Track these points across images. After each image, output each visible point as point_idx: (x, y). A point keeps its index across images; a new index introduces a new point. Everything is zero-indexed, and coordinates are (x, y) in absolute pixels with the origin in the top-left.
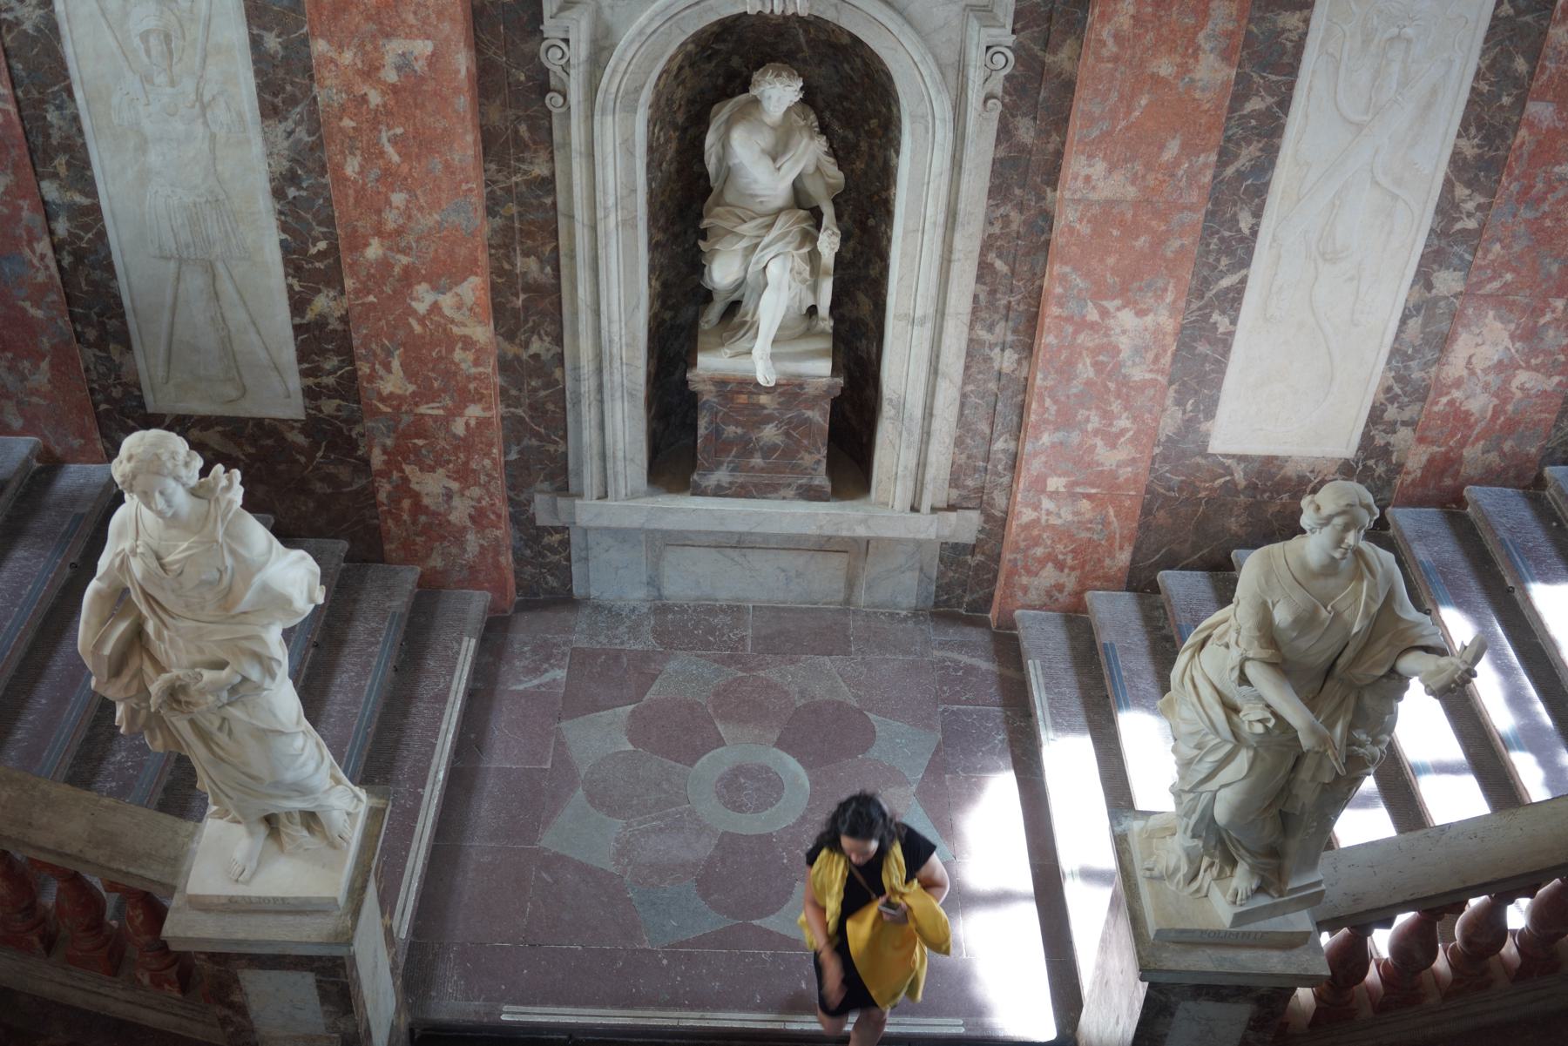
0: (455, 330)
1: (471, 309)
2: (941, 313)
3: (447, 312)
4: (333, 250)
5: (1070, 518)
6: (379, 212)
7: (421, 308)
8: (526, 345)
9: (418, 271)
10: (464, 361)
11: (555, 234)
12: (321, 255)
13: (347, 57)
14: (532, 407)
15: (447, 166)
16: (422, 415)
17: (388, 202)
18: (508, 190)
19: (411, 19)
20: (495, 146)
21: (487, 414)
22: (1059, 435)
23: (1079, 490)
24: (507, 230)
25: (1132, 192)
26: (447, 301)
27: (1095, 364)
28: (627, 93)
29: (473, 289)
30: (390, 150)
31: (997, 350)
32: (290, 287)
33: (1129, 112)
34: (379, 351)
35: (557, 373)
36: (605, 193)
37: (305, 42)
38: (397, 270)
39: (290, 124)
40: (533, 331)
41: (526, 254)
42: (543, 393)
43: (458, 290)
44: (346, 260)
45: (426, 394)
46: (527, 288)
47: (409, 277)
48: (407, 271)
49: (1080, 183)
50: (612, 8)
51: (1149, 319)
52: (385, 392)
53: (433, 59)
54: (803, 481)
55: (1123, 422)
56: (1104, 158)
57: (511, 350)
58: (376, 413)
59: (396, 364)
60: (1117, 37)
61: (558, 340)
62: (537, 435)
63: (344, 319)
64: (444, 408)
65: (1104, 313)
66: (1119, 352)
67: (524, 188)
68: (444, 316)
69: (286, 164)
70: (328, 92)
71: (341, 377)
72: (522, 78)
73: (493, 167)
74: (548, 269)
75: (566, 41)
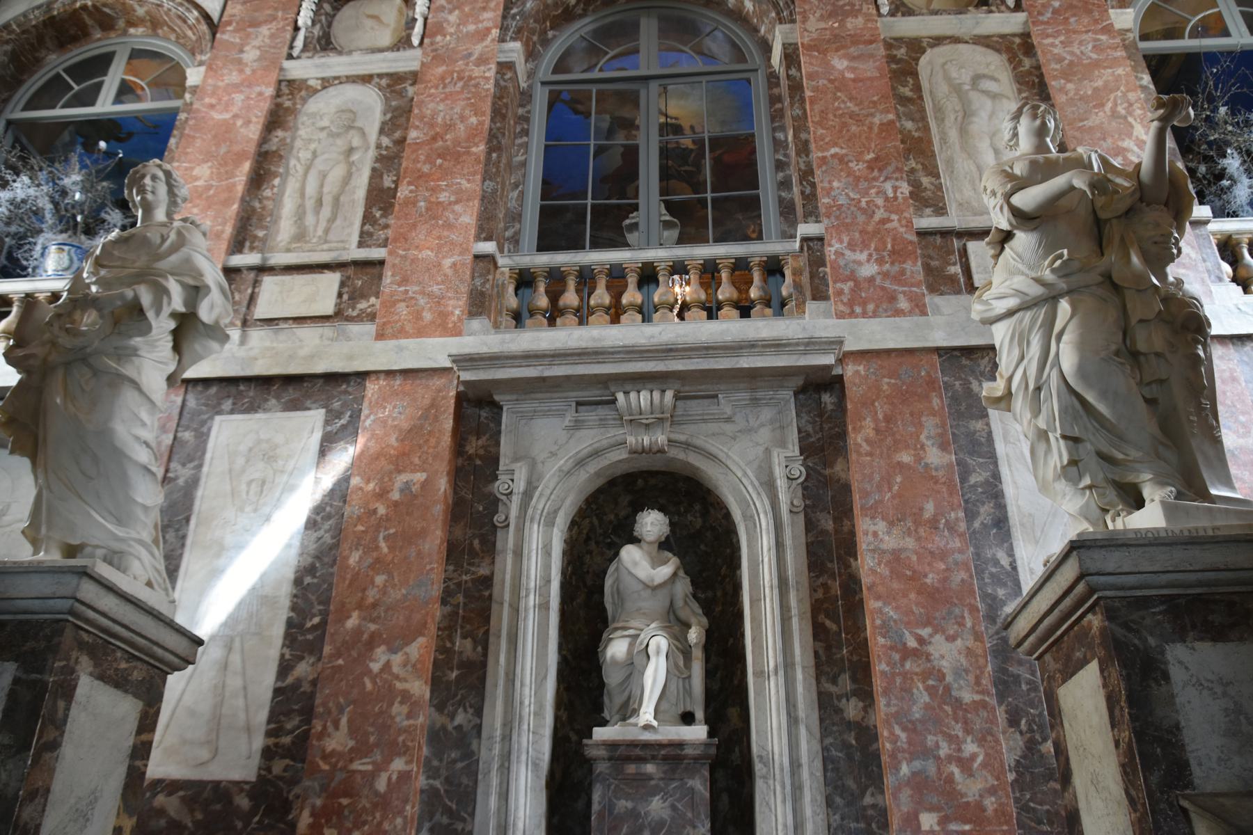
1: (414, 666)
2: (788, 665)
3: (395, 670)
4: (323, 624)
6: (364, 590)
7: (375, 667)
8: (452, 717)
9: (381, 635)
10: (399, 714)
11: (487, 620)
12: (315, 627)
13: (371, 486)
14: (448, 780)
15: (419, 553)
16: (354, 772)
17: (372, 582)
18: (459, 585)
19: (417, 461)
20: (455, 553)
21: (408, 768)
22: (917, 764)
24: (454, 614)
25: (910, 543)
26: (397, 659)
27: (927, 688)
28: (548, 513)
29: (420, 648)
30: (383, 544)
31: (844, 701)
32: (282, 656)
33: (890, 489)
34: (334, 710)
35: (474, 746)
36: (528, 577)
38: (365, 636)
39: (322, 532)
40: (461, 703)
41: (464, 637)
42: (460, 765)
43: (407, 649)
44: (331, 629)
45: (361, 750)
46: (462, 665)
47: (371, 644)
49: (870, 538)
51: (959, 642)
53: (425, 485)
55: (970, 747)
56: (883, 519)
57: (440, 720)
59: (344, 721)
60: (867, 440)
61: (479, 712)
62: (448, 812)
63: (314, 683)
64: (373, 763)
65: (921, 641)
66: (944, 676)
69: (310, 560)
71: (297, 737)
73: (451, 568)
74: (479, 649)
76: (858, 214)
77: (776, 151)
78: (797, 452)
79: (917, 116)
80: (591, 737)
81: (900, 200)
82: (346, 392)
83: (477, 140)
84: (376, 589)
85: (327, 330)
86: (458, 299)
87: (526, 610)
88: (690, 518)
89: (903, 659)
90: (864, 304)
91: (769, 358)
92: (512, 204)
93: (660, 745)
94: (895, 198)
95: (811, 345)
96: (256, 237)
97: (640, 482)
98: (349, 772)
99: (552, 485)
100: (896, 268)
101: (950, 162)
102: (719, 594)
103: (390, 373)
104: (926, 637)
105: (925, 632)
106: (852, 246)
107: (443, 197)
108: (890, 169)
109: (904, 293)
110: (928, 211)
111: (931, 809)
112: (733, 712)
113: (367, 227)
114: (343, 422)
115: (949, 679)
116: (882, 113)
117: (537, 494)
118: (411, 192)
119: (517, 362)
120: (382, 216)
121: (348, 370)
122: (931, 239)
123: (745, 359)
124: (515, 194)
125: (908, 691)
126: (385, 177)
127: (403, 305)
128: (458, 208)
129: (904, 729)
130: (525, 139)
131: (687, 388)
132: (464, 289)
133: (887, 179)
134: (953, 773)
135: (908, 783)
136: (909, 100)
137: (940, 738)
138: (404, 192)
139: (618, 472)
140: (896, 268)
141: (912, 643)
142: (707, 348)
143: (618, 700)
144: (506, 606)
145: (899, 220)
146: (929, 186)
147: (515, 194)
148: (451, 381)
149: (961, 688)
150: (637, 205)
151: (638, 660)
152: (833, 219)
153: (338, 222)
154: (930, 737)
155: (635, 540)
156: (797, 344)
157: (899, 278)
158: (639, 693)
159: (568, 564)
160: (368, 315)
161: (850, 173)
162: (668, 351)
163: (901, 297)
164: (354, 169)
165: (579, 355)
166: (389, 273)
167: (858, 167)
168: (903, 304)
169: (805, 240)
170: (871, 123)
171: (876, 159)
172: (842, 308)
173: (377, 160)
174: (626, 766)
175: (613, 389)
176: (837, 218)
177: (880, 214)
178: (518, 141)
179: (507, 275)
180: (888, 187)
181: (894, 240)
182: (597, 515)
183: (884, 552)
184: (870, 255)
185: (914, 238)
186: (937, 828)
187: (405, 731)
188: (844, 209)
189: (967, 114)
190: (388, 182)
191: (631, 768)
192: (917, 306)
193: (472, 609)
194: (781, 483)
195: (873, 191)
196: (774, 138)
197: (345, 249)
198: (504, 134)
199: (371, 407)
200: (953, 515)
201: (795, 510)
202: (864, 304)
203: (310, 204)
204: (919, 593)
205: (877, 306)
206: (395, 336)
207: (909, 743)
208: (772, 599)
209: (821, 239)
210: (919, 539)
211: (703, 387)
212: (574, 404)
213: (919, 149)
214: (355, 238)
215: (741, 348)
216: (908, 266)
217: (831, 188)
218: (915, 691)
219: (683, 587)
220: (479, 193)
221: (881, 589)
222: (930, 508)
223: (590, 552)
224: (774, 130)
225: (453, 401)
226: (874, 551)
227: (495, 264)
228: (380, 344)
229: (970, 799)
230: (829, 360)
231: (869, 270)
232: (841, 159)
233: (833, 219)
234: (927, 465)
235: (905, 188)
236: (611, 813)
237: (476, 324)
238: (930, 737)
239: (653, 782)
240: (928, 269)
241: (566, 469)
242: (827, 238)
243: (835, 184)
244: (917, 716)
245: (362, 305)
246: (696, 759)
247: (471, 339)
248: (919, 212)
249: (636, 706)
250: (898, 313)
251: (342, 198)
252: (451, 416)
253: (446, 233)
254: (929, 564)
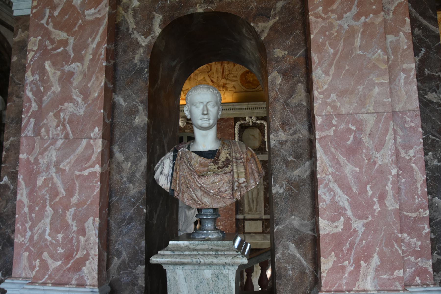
96: (240, 210)
153: (258, 206)
203: (251, 201)
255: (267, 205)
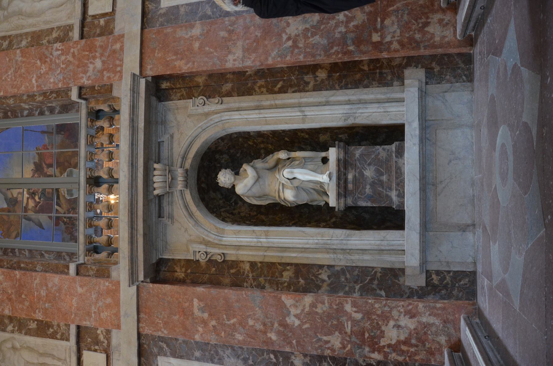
0: (307, 309)
1: (297, 302)
2: (300, 105)
3: (299, 312)
4: (274, 352)
5: (396, 27)
6: (256, 331)
7: (297, 322)
8: (323, 281)
9: (281, 320)
10: (322, 308)
11: (273, 264)
12: (276, 357)
13: (200, 329)
14: (355, 282)
15: (237, 301)
16: (351, 331)
17: (252, 326)
18: (254, 280)
19: (187, 304)
20: (237, 283)
21: (350, 302)
22: (349, 42)
23: (379, 26)
24: (270, 282)
25: (240, 43)
26: (293, 311)
28: (218, 232)
29: (288, 300)
30: (232, 321)
31: (317, 79)
33: (212, 53)
34: (319, 344)
35: (338, 268)
36: (251, 242)
37: (197, 343)
39: (225, 355)
40: (316, 277)
41: (282, 276)
42: (348, 276)
43: (288, 306)
44: (277, 348)
45: (340, 328)
46: (297, 277)
47: (284, 325)
48: (281, 325)
49: (236, 63)
50: (190, 236)
52: (340, 346)
53: (200, 300)
54: (394, 155)
56: (227, 56)
57: (325, 287)
58: (351, 353)
59: (325, 338)
60: (186, 64)
61: (321, 267)
62: (372, 280)
63: (305, 356)
64: (347, 321)
65: (289, 39)
66: (306, 28)
67: (254, 274)
68: (301, 313)
69: (240, 361)
70: (213, 339)
72: (214, 269)
73: (245, 284)
74: (288, 268)
75: (199, 252)
76: (68, 68)
77: (34, 115)
78: (191, 100)
79: (19, 38)
80: (335, 208)
81: (63, 47)
82: (148, 345)
83: (12, 275)
84: (256, 324)
85: (115, 357)
86: (100, 284)
87: (268, 243)
88: (223, 161)
89: (298, 47)
90: (116, 66)
91: (140, 113)
92: (52, 256)
93: (339, 171)
94: (62, 50)
95: (134, 90)
97: (203, 185)
98: (352, 334)
99: (202, 230)
100: (99, 50)
101: (46, 22)
102: (262, 146)
103: (139, 321)
104: (287, 36)
105: (285, 37)
106: (85, 72)
107: (43, 293)
108: (46, 53)
109: (112, 46)
110: (70, 34)
111: (371, 36)
112: (323, 138)
113: (58, 336)
114: (165, 346)
115: (308, 26)
116: (16, 56)
117: (206, 238)
118: (39, 312)
119: (135, 249)
120: (52, 328)
121: (136, 344)
122: (85, 32)
123: (139, 125)
124: (46, 255)
125: (313, 45)
126: (30, 327)
127: (102, 314)
128: (50, 285)
129: (332, 48)
130: (16, 251)
131: (154, 158)
132: (94, 280)
133: (51, 54)
134: (354, 25)
135: (358, 46)
136: (10, 43)
137: (336, 31)
138: (39, 316)
139: (197, 195)
140: (99, 50)
141: (290, 43)
142: (132, 144)
143: (316, 196)
144: (266, 254)
145: (74, 48)
146: (57, 34)
147: (46, 255)
148: (144, 286)
149: (312, 21)
150: (56, 189)
151: (296, 183)
152: (70, 82)
153: (55, 353)
154: (336, 36)
155: (234, 187)
156: (133, 97)
157: (104, 48)
158: (312, 184)
159: (245, 223)
160: (107, 334)
161: (47, 73)
162: (133, 165)
163: (114, 47)
164: (25, 345)
165: (132, 214)
166: (84, 323)
167: (44, 69)
168: (118, 46)
169: (80, 96)
170: (21, 61)
171: (40, 59)
172: (117, 77)
173: (21, 332)
174: (349, 189)
175: (152, 197)
176: (70, 79)
177: (70, 58)
178: (17, 254)
179: (89, 258)
180: (56, 53)
181: (84, 51)
182: (220, 209)
183: (244, 56)
184: (91, 63)
185: (84, 41)
186: (379, 34)
187: (331, 305)
188: (65, 76)
189: (20, 13)
190: (33, 325)
191: (350, 186)
192: (119, 39)
193: (268, 274)
194: (207, 109)
195: (57, 61)
196: (26, 116)
197: (70, 349)
198: (11, 260)
199: (158, 330)
200: (227, 23)
201: (220, 102)
202: (116, 66)
204: (265, 39)
205: (118, 59)
206: (119, 319)
207: (339, 45)
208: (266, 113)
209: (80, 88)
210: (238, 39)
211: (154, 149)
212: (160, 219)
213: (36, 38)
214: (64, 343)
215: (133, 126)
216: (98, 44)
217: (54, 82)
218: (313, 42)
219: (258, 163)
220: (42, 273)
221: (263, 58)
222: (223, 34)
223: (239, 213)
224: (22, 116)
225: (155, 285)
226: (243, 61)
227: (82, 264)
228: (123, 327)
229: (366, 18)
230: (143, 82)
231: (98, 64)
232: (39, 77)
233: (70, 82)
234: (201, 35)
235: (58, 45)
236: (372, 197)
237: (114, 274)
238: (336, 36)
239: (357, 175)
240: (100, 35)
241: (194, 223)
242: (80, 84)
243: (52, 80)
244: (326, 41)
245: (101, 337)
246: (346, 153)
247: (121, 275)
248: (69, 39)
249: (319, 186)
250: (122, 49)
251: (41, 352)
252: (163, 285)
253: (64, 291)
254: (251, 34)
255: (51, 330)
